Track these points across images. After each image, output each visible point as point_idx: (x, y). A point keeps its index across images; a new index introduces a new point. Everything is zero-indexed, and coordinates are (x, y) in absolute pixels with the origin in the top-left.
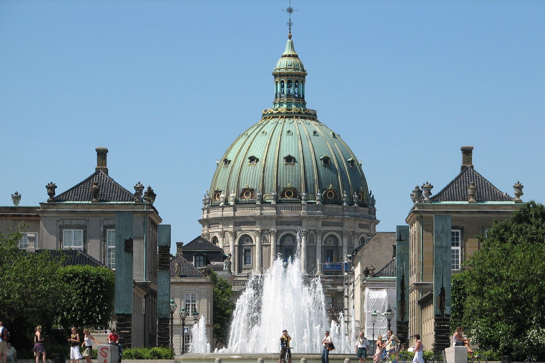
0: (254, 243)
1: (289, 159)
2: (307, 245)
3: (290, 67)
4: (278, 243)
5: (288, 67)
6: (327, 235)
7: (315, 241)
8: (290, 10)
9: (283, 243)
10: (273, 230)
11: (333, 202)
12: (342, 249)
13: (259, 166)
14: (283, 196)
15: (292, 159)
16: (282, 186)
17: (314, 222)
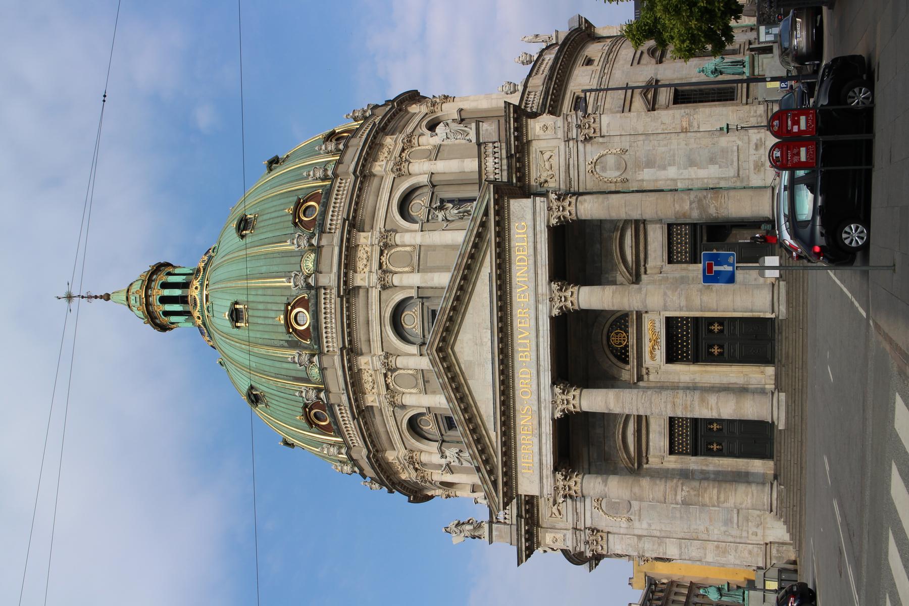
0: (424, 411)
1: (236, 315)
2: (418, 272)
3: (138, 299)
4: (413, 349)
5: (138, 303)
6: (398, 217)
7: (408, 249)
8: (69, 297)
9: (416, 336)
10: (378, 365)
11: (323, 206)
12: (438, 173)
13: (262, 387)
14: (303, 334)
15: (236, 309)
16: (287, 337)
17: (361, 254)
